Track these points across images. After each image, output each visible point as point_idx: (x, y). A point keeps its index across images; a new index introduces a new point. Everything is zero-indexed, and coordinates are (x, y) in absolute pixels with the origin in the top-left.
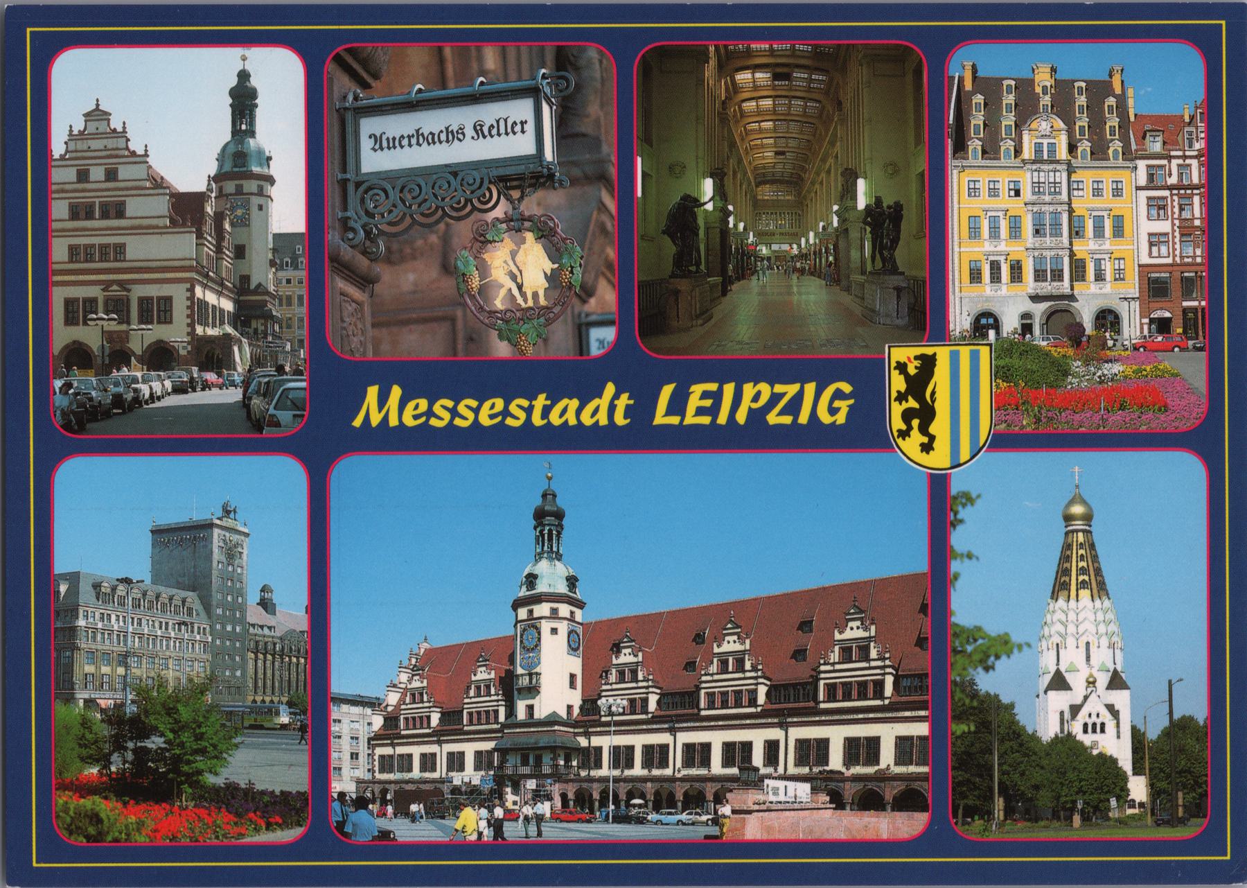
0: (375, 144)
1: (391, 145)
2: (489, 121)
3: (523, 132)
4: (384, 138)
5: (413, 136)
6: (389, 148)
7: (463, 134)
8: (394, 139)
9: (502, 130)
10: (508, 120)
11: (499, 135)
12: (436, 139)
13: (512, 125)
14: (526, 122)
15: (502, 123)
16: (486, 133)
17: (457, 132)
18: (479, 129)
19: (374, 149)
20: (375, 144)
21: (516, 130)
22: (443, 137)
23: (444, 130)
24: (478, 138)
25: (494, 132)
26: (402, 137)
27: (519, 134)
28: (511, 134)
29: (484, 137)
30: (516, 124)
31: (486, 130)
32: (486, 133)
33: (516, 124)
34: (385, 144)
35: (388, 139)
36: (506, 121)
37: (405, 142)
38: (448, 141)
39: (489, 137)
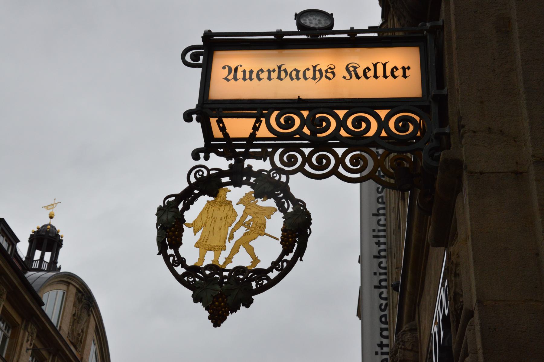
0: (229, 73)
1: (247, 76)
3: (405, 76)
5: (274, 71)
6: (244, 79)
7: (333, 73)
8: (251, 72)
10: (387, 64)
12: (301, 75)
13: (392, 70)
14: (409, 68)
16: (361, 73)
17: (326, 71)
19: (227, 79)
20: (229, 73)
21: (396, 74)
22: (309, 74)
23: (311, 69)
24: (351, 77)
25: (370, 74)
26: (262, 71)
27: (400, 78)
28: (391, 78)
29: (358, 77)
30: (397, 69)
31: (360, 72)
32: (361, 73)
35: (244, 72)
36: (384, 65)
37: (264, 75)
38: (314, 78)
39: (363, 78)
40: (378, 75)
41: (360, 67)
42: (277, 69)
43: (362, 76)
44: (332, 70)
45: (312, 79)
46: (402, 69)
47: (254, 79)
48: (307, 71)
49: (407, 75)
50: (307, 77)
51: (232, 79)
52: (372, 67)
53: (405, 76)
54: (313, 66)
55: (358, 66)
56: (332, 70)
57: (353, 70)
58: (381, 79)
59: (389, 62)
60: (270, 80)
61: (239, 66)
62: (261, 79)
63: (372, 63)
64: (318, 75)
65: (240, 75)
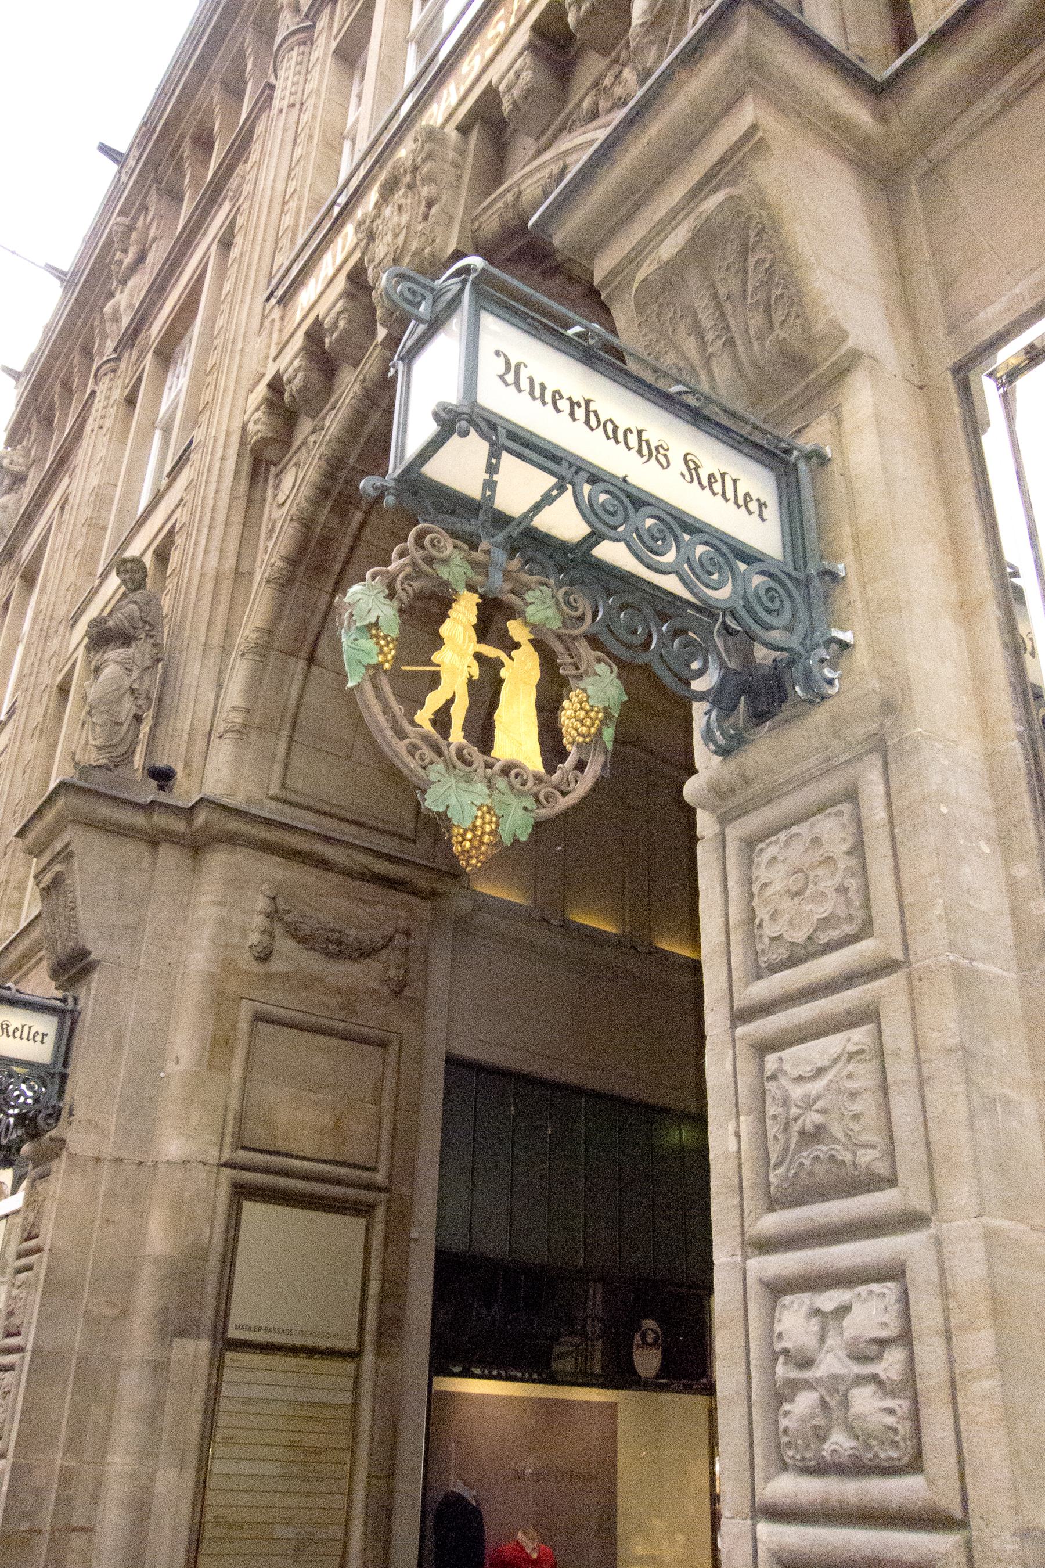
1: (537, 393)
7: (665, 456)
9: (25, 1035)
10: (738, 483)
15: (26, 1029)
19: (501, 377)
24: (692, 481)
36: (735, 481)
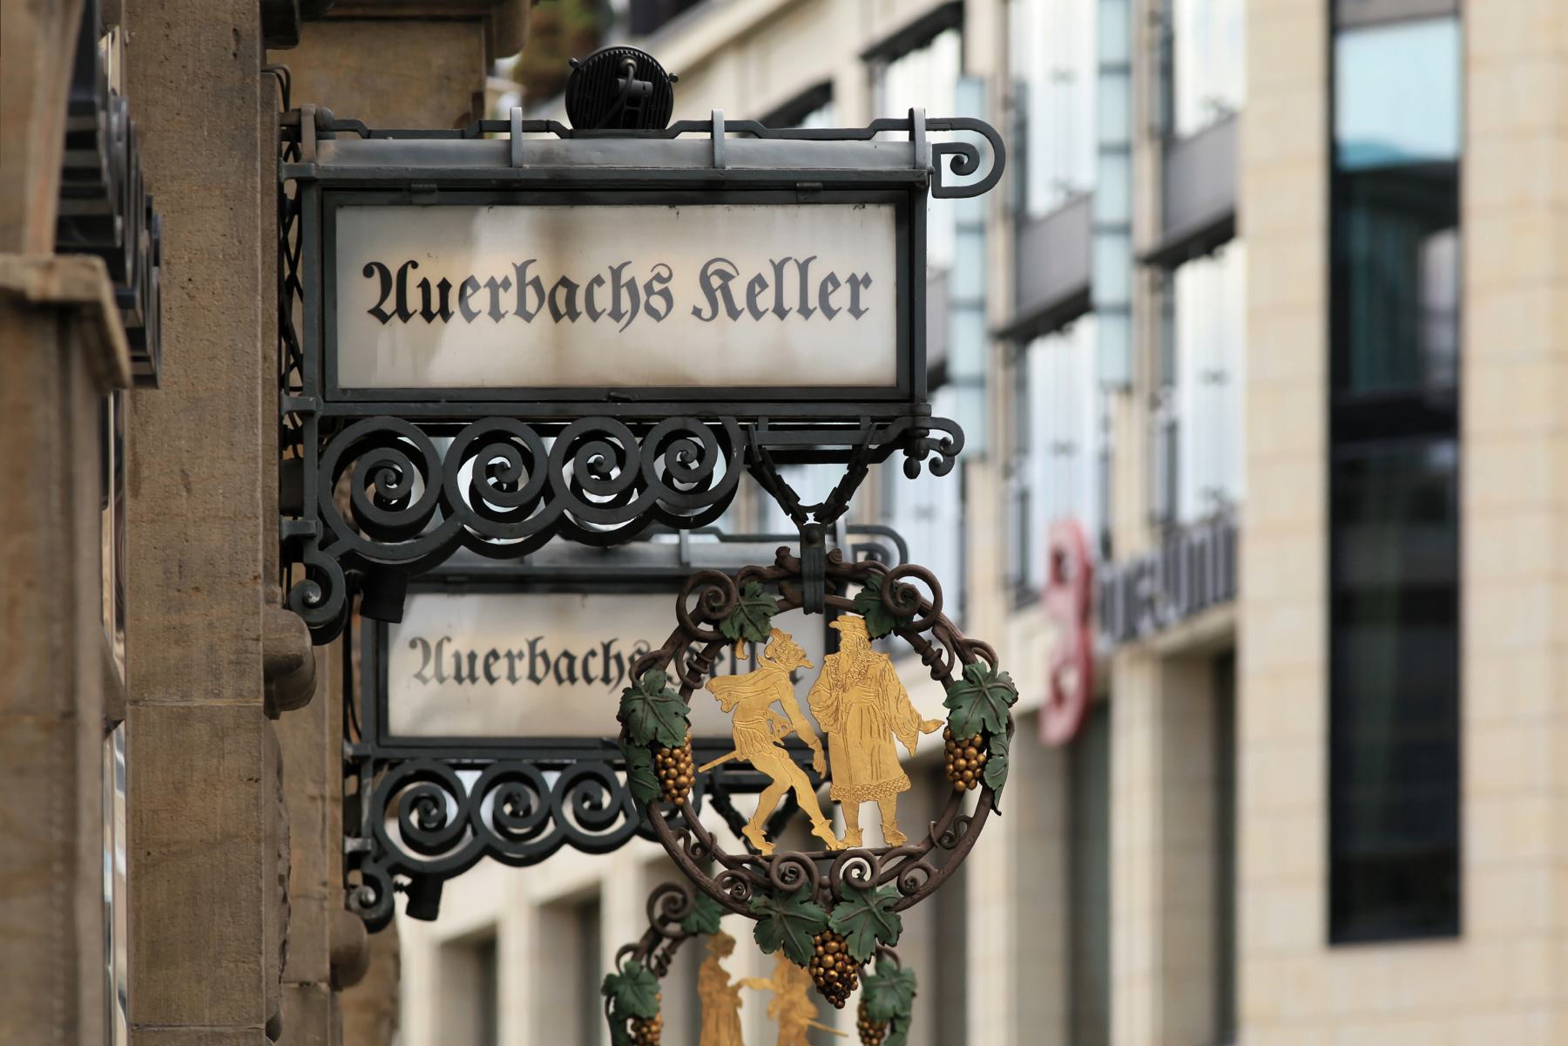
1: (435, 305)
2: (750, 263)
3: (856, 311)
4: (413, 278)
6: (428, 315)
7: (666, 295)
8: (445, 286)
10: (811, 265)
11: (781, 312)
14: (867, 281)
17: (649, 289)
18: (715, 285)
19: (377, 313)
25: (766, 300)
27: (844, 317)
28: (818, 315)
29: (734, 313)
30: (836, 285)
32: (740, 301)
33: (836, 285)
34: (414, 300)
35: (425, 285)
36: (803, 268)
39: (746, 316)
40: (786, 306)
41: (738, 274)
42: (513, 279)
43: (743, 309)
44: (663, 286)
45: (609, 315)
46: (848, 284)
47: (453, 312)
48: (595, 286)
49: (862, 307)
50: (599, 309)
51: (393, 314)
52: (770, 278)
53: (856, 311)
54: (610, 268)
55: (730, 270)
56: (663, 286)
57: (720, 287)
58: (794, 317)
59: (815, 257)
60: (497, 320)
61: (410, 266)
62: (475, 315)
63: (771, 261)
64: (626, 304)
65: (414, 300)
